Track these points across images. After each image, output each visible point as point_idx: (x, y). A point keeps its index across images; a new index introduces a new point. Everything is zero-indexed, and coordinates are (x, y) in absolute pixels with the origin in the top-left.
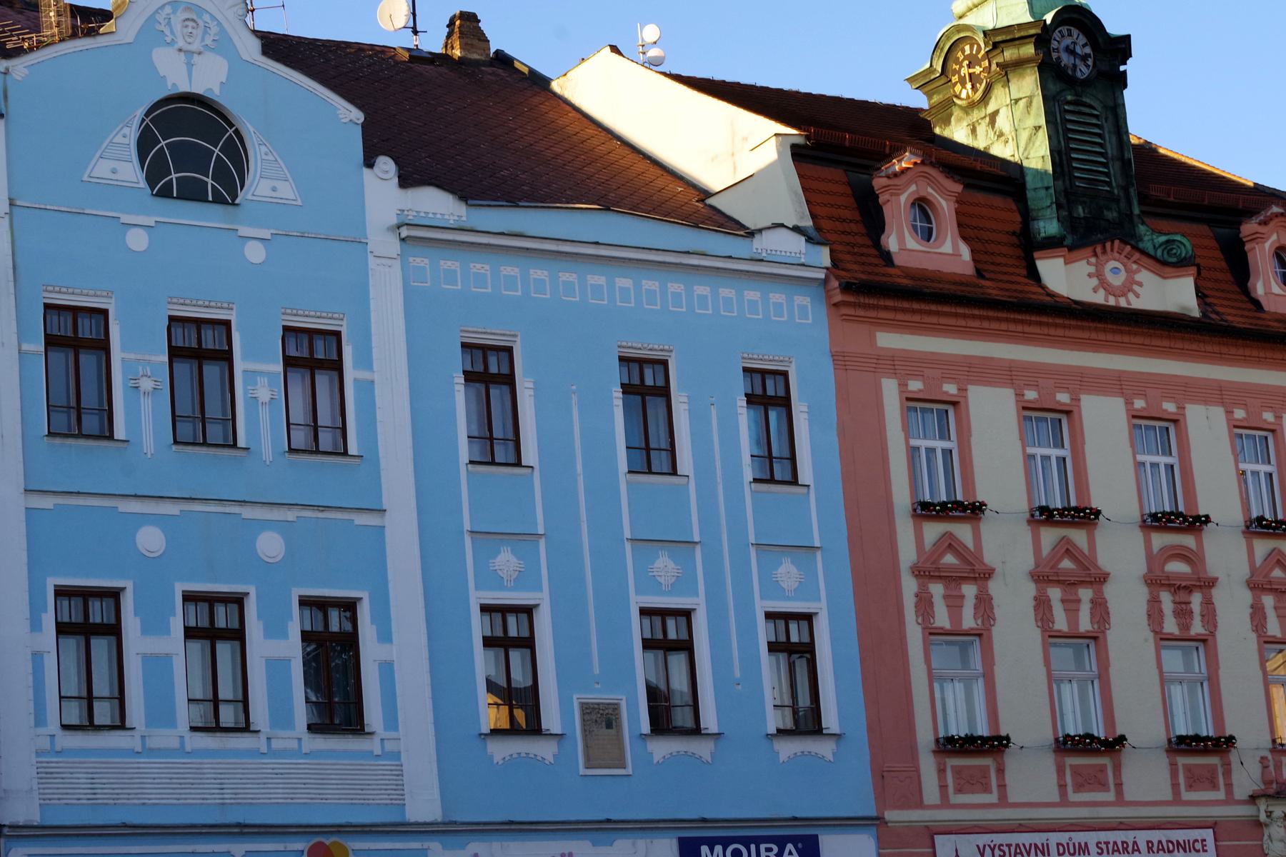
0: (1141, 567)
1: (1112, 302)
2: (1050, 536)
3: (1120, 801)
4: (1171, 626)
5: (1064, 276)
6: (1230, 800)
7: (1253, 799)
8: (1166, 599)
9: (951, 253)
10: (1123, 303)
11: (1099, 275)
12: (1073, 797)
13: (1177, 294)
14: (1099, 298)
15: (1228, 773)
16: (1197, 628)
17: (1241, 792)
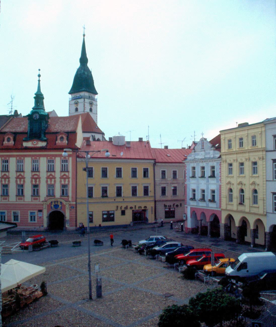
0: (31, 176)
1: (34, 146)
2: (18, 174)
3: (24, 201)
4: (34, 183)
5: (25, 144)
6: (39, 201)
7: (43, 201)
8: (34, 180)
9: (12, 143)
10: (36, 146)
11: (33, 144)
12: (18, 201)
13: (43, 144)
14: (32, 146)
15: (39, 198)
16: (37, 183)
17: (41, 200)
